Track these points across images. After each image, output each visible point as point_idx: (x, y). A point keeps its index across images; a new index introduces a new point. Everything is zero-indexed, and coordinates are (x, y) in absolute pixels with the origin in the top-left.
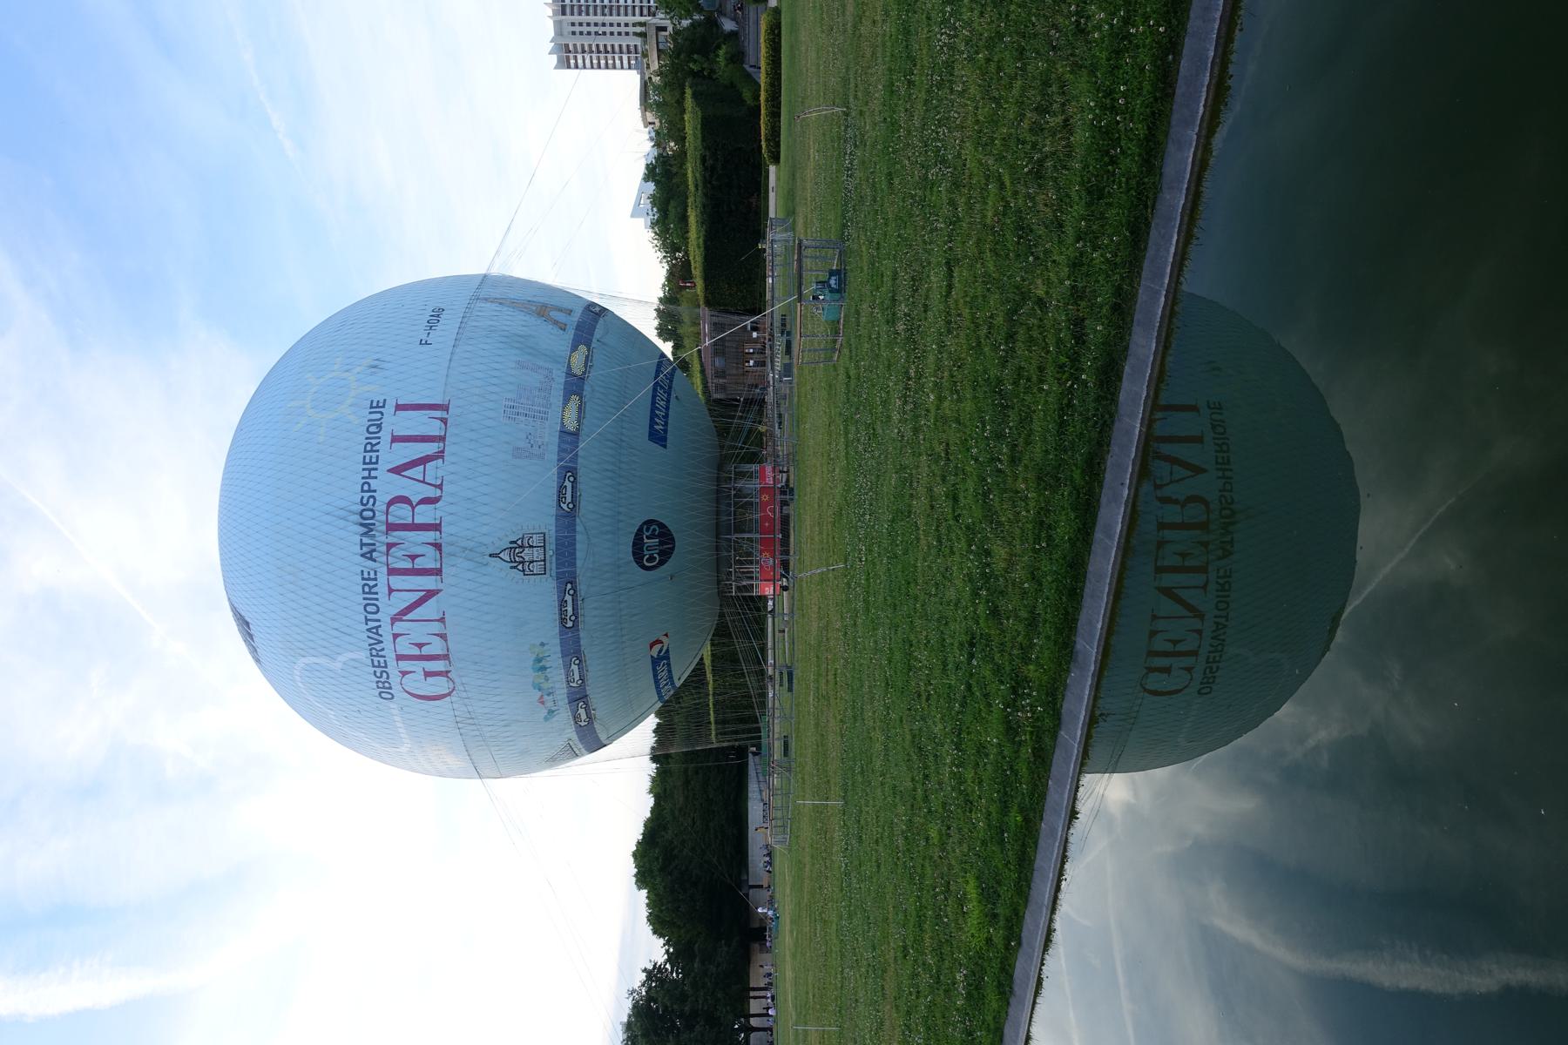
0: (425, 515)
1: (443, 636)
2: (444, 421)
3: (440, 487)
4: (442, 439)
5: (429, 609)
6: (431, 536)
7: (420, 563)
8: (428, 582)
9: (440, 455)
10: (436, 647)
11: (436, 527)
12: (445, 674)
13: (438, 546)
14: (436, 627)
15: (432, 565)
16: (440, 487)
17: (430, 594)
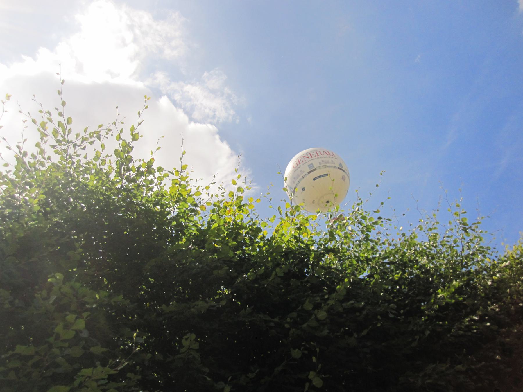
0: (319, 154)
1: (303, 161)
2: (333, 156)
3: (324, 155)
4: (330, 155)
5: (306, 158)
6: (316, 155)
7: (312, 155)
8: (310, 157)
9: (328, 155)
10: (300, 162)
11: (318, 155)
12: (297, 165)
13: (315, 156)
14: (304, 160)
15: (313, 156)
16: (324, 155)
17: (308, 158)
